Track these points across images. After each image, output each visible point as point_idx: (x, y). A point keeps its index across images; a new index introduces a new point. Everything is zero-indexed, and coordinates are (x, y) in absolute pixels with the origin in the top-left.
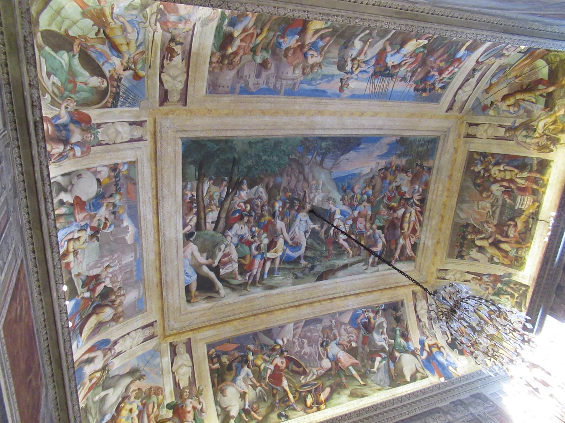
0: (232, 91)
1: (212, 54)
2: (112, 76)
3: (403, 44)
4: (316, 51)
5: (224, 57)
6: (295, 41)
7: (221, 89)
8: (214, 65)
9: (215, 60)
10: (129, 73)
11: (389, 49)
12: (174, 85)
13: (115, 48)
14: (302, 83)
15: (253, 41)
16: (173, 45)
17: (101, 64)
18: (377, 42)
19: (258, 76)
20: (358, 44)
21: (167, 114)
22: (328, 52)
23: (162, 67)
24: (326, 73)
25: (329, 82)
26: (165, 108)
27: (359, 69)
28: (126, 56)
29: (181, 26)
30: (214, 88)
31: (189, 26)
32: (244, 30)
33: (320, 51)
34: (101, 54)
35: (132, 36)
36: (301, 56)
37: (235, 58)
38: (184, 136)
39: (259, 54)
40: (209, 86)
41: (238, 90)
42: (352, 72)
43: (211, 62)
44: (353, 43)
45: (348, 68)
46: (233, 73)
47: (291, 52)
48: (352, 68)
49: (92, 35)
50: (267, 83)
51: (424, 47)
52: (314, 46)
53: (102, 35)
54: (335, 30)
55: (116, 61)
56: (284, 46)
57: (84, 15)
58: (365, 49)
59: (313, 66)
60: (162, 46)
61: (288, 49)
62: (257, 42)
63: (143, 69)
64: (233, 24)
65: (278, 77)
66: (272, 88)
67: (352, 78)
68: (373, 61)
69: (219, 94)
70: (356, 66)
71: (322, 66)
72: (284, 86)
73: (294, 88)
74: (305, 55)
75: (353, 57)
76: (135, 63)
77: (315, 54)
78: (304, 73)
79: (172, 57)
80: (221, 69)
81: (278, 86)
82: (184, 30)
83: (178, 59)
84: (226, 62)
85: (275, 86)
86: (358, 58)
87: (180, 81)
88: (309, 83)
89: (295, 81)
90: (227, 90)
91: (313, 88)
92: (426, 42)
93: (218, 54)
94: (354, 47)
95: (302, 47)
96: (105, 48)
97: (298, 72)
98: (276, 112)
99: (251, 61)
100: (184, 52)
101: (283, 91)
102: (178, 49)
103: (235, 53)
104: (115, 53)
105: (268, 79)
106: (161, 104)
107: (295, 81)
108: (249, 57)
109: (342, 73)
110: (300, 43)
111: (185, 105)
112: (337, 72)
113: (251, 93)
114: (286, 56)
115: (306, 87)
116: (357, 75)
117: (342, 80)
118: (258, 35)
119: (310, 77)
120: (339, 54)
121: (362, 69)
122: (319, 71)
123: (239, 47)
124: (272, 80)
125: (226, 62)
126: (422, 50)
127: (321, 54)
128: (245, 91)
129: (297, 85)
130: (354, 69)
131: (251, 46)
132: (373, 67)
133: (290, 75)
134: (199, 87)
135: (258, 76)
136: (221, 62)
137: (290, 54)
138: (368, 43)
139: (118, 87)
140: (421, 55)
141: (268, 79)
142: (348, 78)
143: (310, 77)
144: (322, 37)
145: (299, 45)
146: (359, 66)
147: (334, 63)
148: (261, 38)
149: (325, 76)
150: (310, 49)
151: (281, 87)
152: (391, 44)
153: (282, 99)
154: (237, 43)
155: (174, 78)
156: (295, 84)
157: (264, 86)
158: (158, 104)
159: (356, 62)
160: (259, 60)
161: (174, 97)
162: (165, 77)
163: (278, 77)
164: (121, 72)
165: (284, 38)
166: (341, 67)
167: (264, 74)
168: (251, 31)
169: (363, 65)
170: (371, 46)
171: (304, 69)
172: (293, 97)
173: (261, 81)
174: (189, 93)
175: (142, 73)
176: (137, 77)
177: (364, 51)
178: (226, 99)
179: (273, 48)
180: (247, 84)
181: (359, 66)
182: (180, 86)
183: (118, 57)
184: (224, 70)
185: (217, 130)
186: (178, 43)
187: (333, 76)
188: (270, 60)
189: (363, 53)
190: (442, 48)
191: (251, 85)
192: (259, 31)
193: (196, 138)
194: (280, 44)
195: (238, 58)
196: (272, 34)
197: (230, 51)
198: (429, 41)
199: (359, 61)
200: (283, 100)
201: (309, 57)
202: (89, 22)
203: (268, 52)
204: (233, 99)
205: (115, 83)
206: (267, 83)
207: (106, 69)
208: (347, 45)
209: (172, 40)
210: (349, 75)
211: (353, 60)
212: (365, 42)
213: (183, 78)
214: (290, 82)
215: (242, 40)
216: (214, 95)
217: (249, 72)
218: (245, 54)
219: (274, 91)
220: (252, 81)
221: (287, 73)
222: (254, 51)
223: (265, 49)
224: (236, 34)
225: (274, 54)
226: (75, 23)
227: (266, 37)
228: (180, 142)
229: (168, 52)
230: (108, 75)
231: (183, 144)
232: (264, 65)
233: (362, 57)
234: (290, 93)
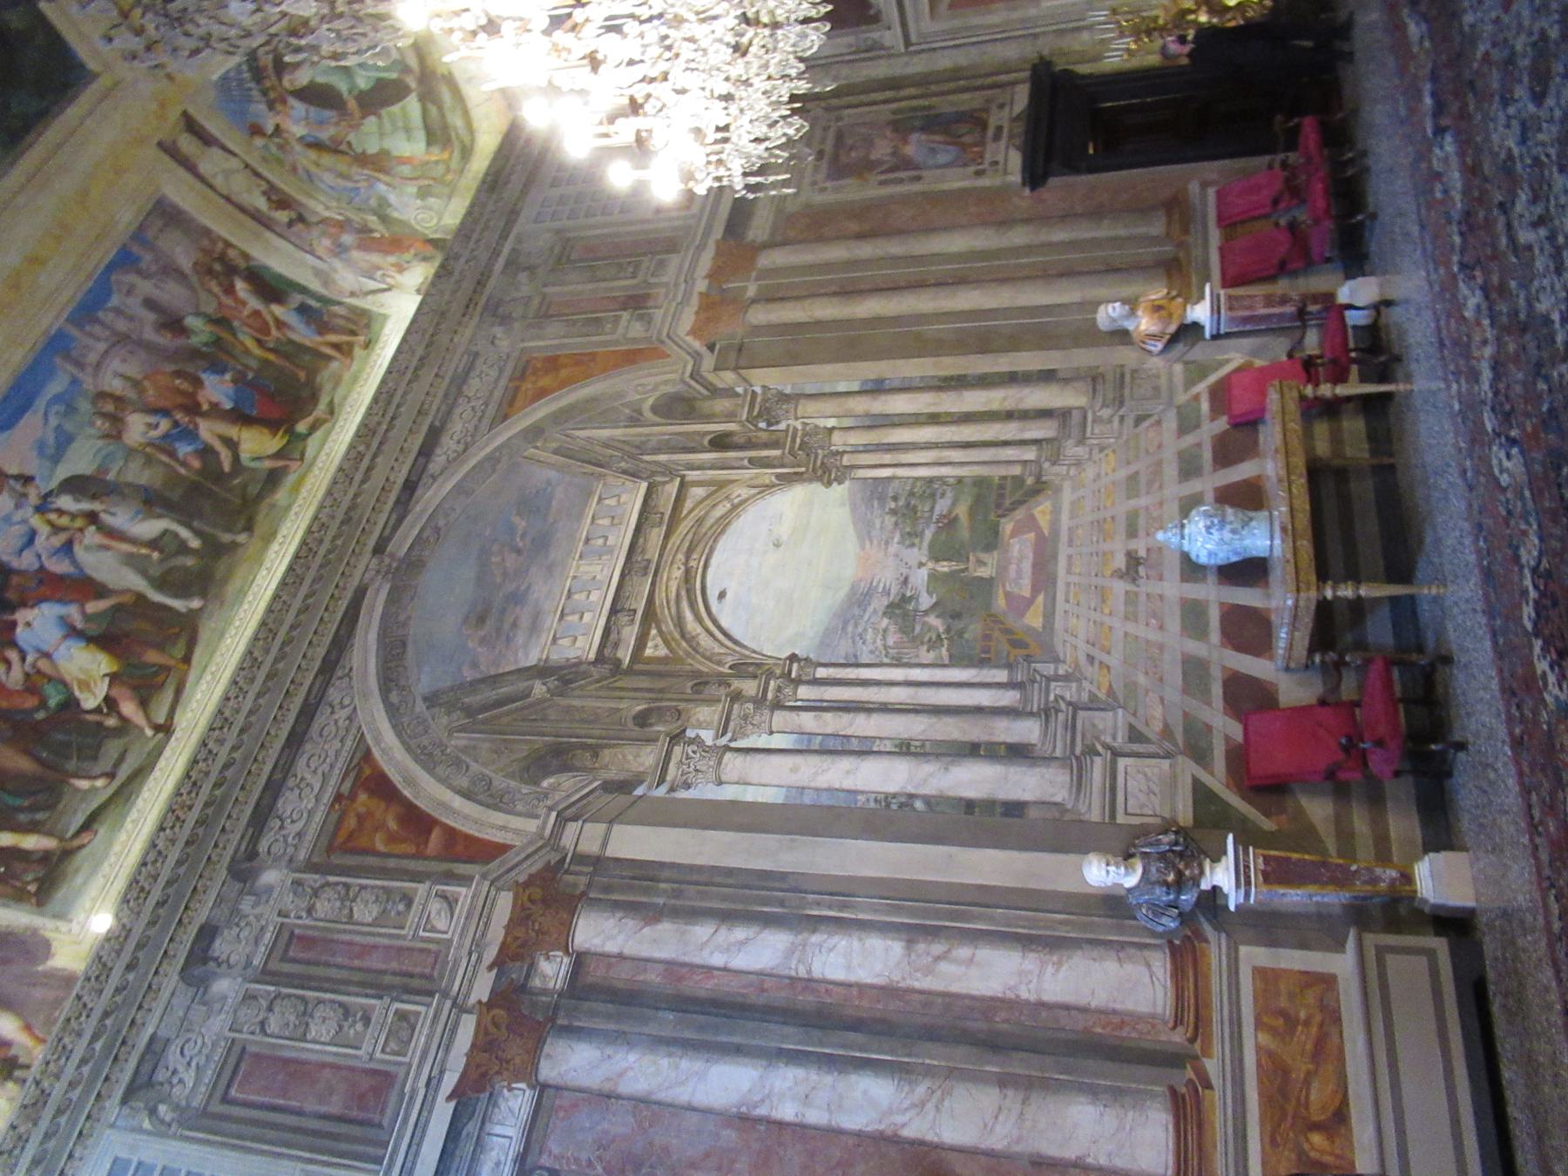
0: (139, 235)
1: (246, 256)
2: (284, 102)
3: (105, 641)
4: (166, 436)
5: (231, 270)
6: (214, 399)
7: (159, 223)
8: (220, 245)
9: (231, 253)
10: (270, 129)
11: (93, 607)
12: (211, 163)
13: (317, 145)
14: (75, 381)
15: (246, 329)
16: (293, 215)
17: (312, 109)
18: (144, 573)
19: (150, 303)
20: (151, 528)
21: (163, 106)
22: (149, 460)
23: (257, 175)
24: (75, 445)
25: (41, 447)
26: (174, 114)
27: (44, 530)
28: (298, 148)
29: (327, 242)
30: (167, 214)
31: (320, 251)
32: (280, 324)
33: (165, 445)
34: (321, 123)
35: (329, 178)
36: (162, 403)
37: (220, 285)
38: (94, 86)
39: (209, 328)
40: (174, 206)
41: (135, 249)
42: (41, 509)
43: (228, 245)
44: (160, 516)
45: (66, 502)
46: (185, 261)
47: (185, 386)
48: (61, 512)
49: (352, 137)
50: (118, 312)
51: (71, 703)
52: (190, 435)
53: (343, 147)
54: (220, 477)
55: (299, 130)
56: (209, 379)
57: (384, 154)
58: (125, 547)
59: (116, 421)
60: (300, 204)
61: (198, 383)
62: (241, 337)
63: (265, 147)
64: (303, 310)
65: (121, 339)
66: (100, 314)
67: (18, 506)
68: (60, 567)
69: (149, 214)
70: (64, 521)
71: (107, 441)
72: (90, 342)
73: (67, 357)
74: (165, 412)
75: (105, 517)
76: (281, 147)
77: (154, 434)
78: (102, 395)
79: (269, 199)
80: (203, 250)
81: (97, 329)
82: (315, 243)
83: (261, 204)
84: (218, 267)
85: (97, 321)
86: (93, 528)
87: (214, 176)
88: (67, 403)
89: (89, 370)
90: (150, 234)
91: (40, 404)
92: (90, 702)
93: (242, 264)
94: (143, 520)
95: (193, 409)
96: (325, 135)
97: (117, 386)
98: (16, 287)
99: (197, 306)
100: (270, 219)
101: (75, 332)
102: (282, 216)
103: (230, 290)
104: (310, 139)
105: (131, 319)
106: (185, 114)
107: (89, 370)
108: (210, 308)
109: (54, 484)
110: (205, 407)
111: (160, 145)
112: (63, 472)
113: (111, 268)
114: (178, 374)
115: (56, 386)
116: (24, 521)
117: (27, 480)
118: (260, 342)
119: (85, 406)
120: (129, 485)
121: (40, 541)
122: (93, 431)
123: (244, 303)
124: (122, 325)
125: (218, 267)
126: (52, 703)
127: (151, 444)
128: (125, 260)
129: (69, 367)
130: (53, 517)
131: (236, 324)
132: (36, 566)
133: (116, 364)
134: (181, 192)
135: (150, 303)
136: (222, 258)
137: (185, 386)
138: (144, 551)
139: (265, 93)
140: (30, 702)
141: (131, 319)
142: (25, 495)
143: (85, 406)
144: (206, 452)
145: (198, 405)
146: (57, 529)
147: (103, 469)
148: (250, 343)
149: (65, 440)
150: (176, 424)
151: (91, 335)
152: (117, 608)
153: (49, 320)
154: (254, 303)
155: (227, 174)
156: (80, 365)
157: (115, 301)
158: (191, 111)
159: (79, 523)
160: (191, 322)
161: (187, 144)
162: (234, 163)
163: (121, 339)
164: (278, 119)
165: (234, 381)
166: (75, 485)
167: (151, 317)
168: (274, 332)
169: (58, 541)
170: (130, 560)
171: (118, 400)
172: (39, 346)
173: (134, 304)
174: (182, 173)
175: (259, 142)
176: (256, 130)
177: (114, 544)
178: (126, 217)
179: (216, 357)
180: (139, 272)
181: (57, 529)
182: (204, 168)
183: (301, 139)
184: (200, 255)
185: (60, 146)
186: (290, 224)
187: (56, 458)
188: (180, 342)
189: (106, 541)
190: (39, 760)
191: (132, 278)
192: (271, 345)
193: (75, 97)
194: (222, 372)
195: (216, 289)
196: (254, 364)
197: (240, 286)
198: (98, 710)
199: (81, 530)
200: (45, 322)
201: (152, 419)
202: (372, 148)
203: (206, 344)
204: (121, 227)
205: (272, 95)
206: (118, 312)
207: (298, 107)
208: (151, 501)
209: (301, 219)
210: (33, 499)
211: (92, 517)
212: (153, 544)
213: (219, 182)
214: (92, 358)
215: (256, 313)
216: (150, 206)
217: (172, 294)
218: (220, 304)
219: (87, 310)
220: (146, 287)
221: (124, 361)
222: (221, 322)
223: (217, 342)
224: (277, 309)
225: (195, 354)
226: (382, 135)
227: (247, 352)
228: (92, 65)
229: (283, 203)
230: (292, 101)
231: (82, 66)
232: (173, 324)
233: (91, 535)
234: (57, 345)
